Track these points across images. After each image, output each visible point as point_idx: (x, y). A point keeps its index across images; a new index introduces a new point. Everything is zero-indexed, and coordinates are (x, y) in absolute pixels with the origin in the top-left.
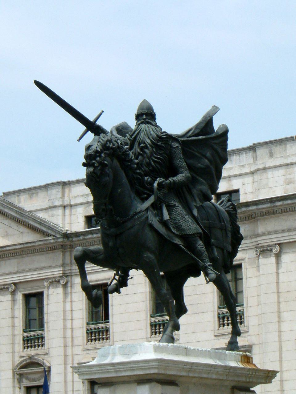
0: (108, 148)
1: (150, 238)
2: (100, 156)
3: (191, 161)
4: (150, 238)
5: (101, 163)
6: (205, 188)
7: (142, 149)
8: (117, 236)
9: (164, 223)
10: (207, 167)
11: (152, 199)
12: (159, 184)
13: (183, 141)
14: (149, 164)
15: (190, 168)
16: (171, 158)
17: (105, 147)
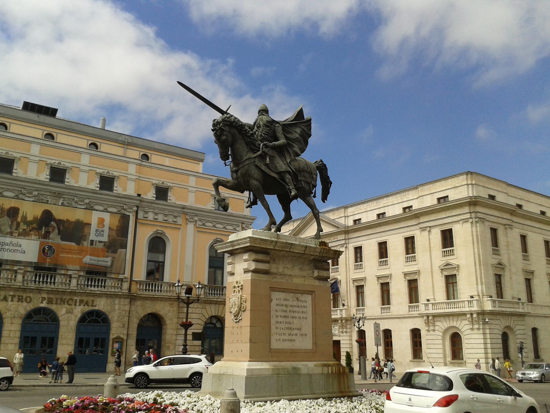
0: (226, 121)
1: (255, 173)
2: (220, 125)
3: (289, 135)
4: (255, 173)
5: (220, 128)
6: (297, 149)
7: (258, 127)
8: (236, 172)
9: (266, 165)
10: (298, 138)
11: (259, 153)
12: (264, 145)
13: (283, 124)
14: (261, 135)
15: (287, 138)
16: (274, 132)
17: (223, 120)
